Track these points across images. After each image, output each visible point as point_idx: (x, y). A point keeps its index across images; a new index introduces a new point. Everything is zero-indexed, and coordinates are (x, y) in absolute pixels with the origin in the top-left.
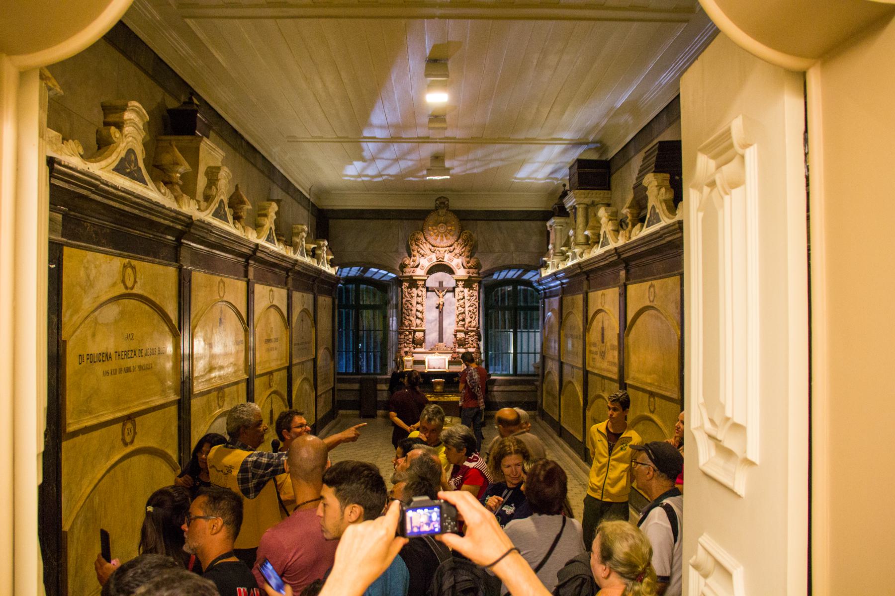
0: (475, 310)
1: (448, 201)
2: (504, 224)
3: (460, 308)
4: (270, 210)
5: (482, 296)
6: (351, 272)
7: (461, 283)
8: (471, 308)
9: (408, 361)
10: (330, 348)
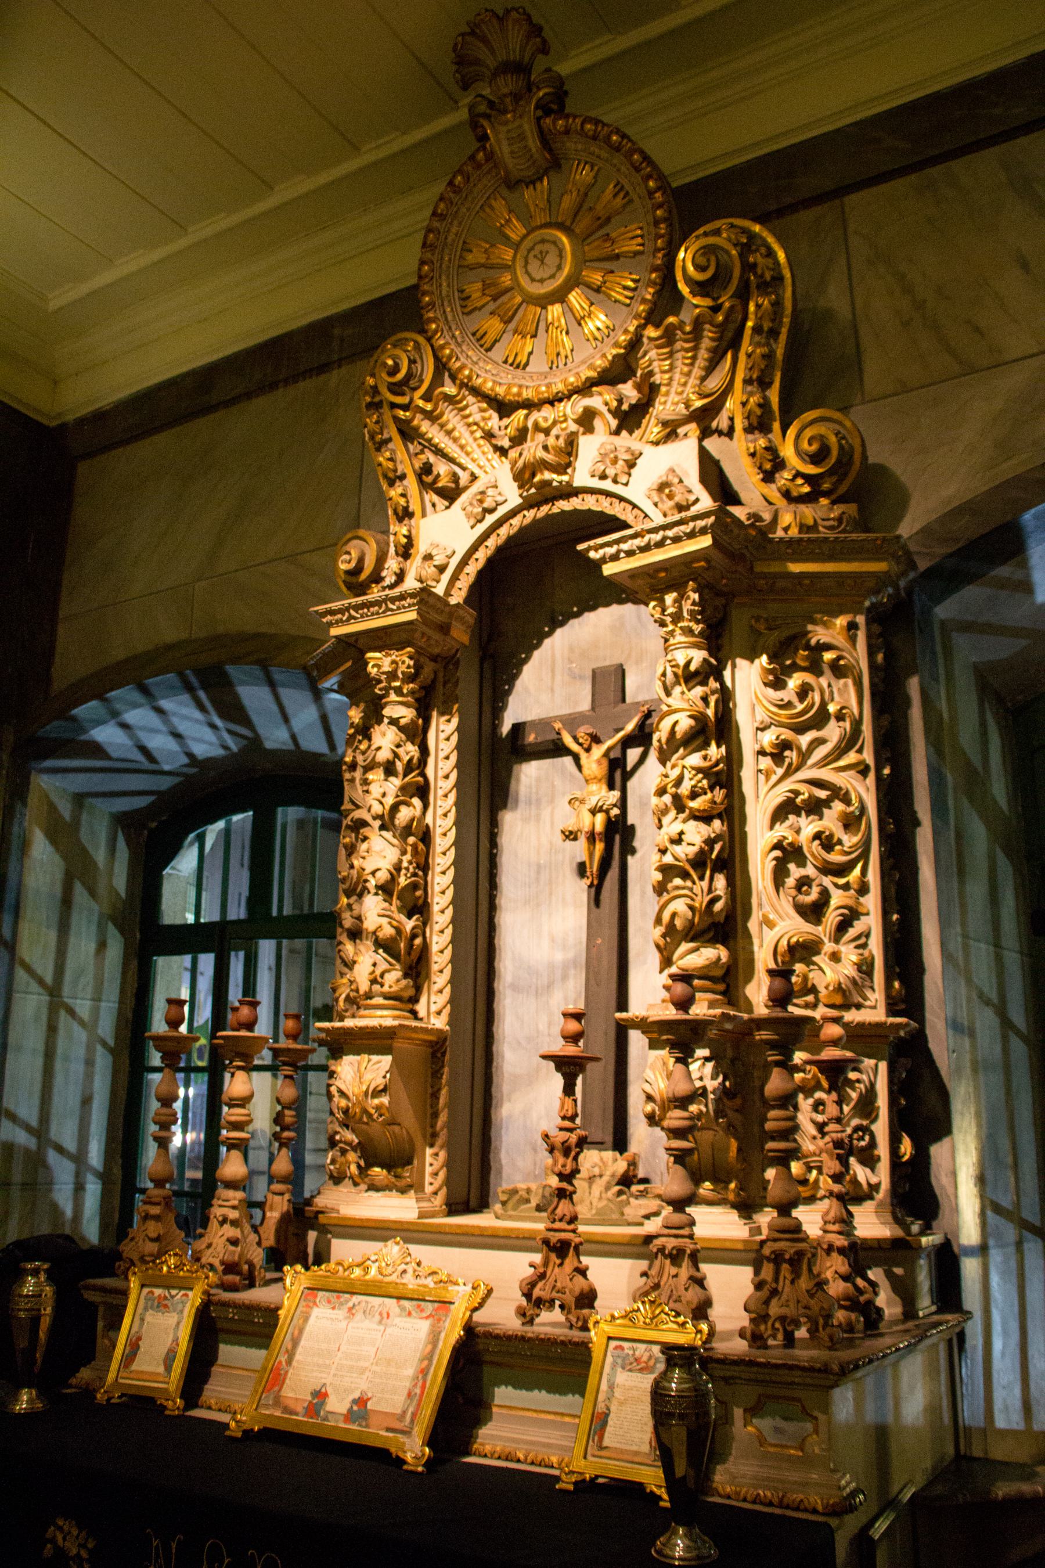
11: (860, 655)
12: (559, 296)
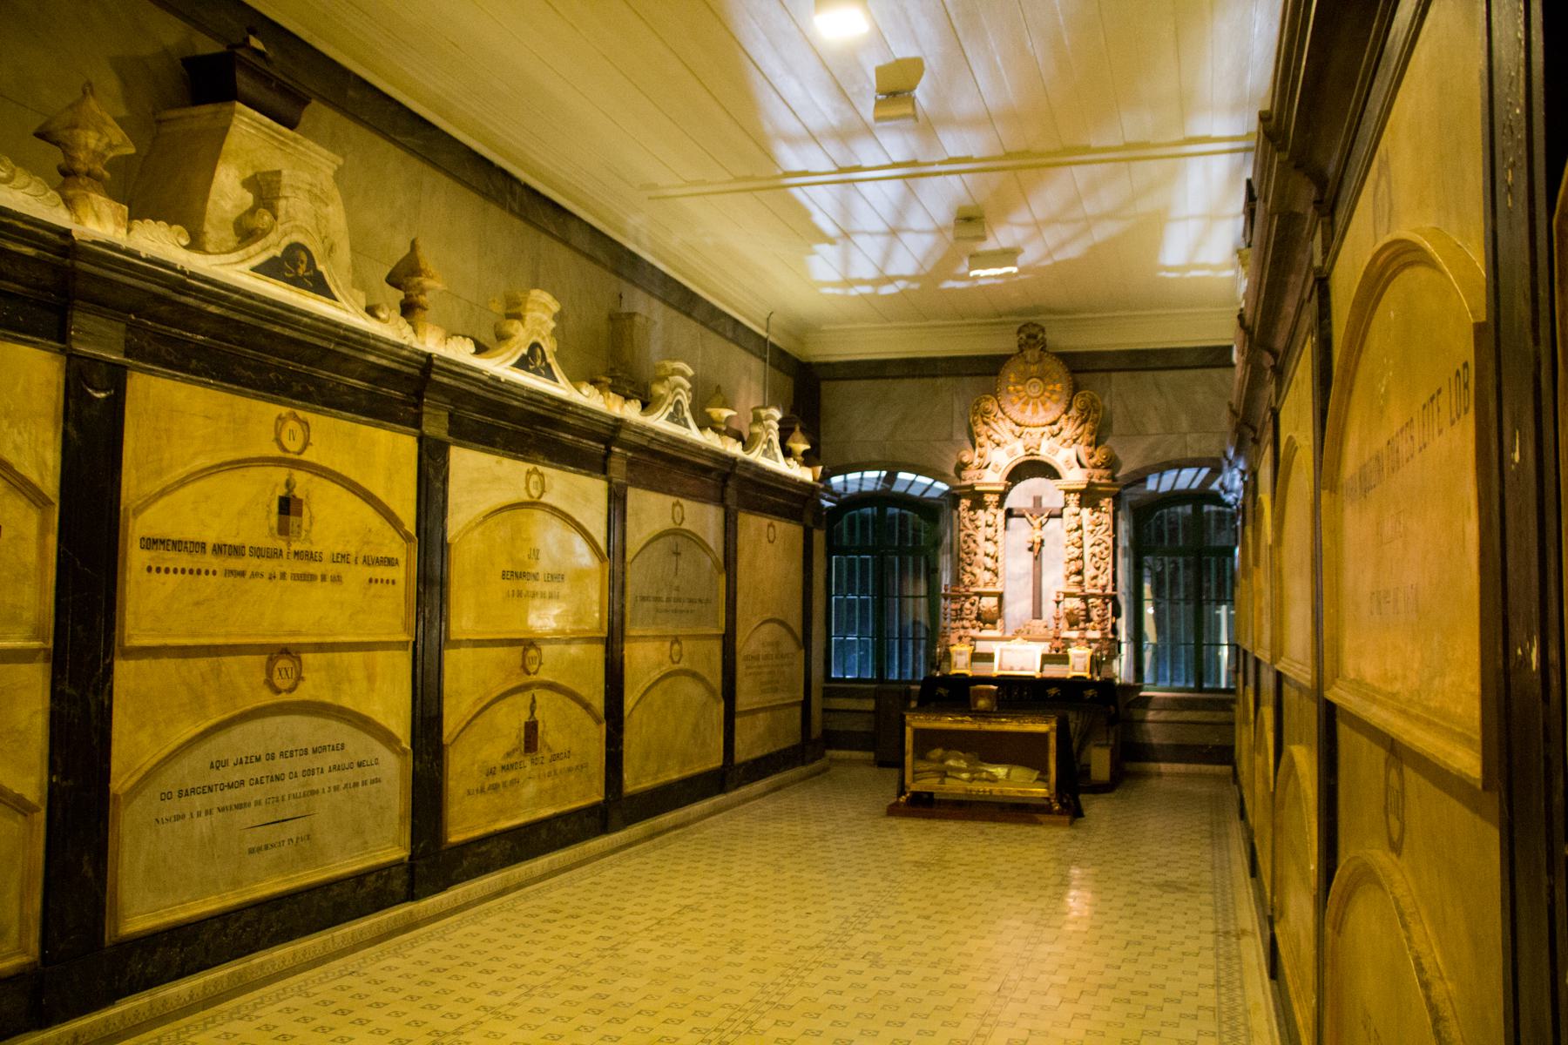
0: (1106, 552)
1: (1043, 330)
2: (1167, 377)
3: (1072, 549)
4: (529, 306)
5: (1123, 526)
6: (865, 483)
7: (1074, 498)
8: (1097, 550)
9: (960, 654)
10: (796, 623)
11: (1110, 508)
12: (1038, 397)
